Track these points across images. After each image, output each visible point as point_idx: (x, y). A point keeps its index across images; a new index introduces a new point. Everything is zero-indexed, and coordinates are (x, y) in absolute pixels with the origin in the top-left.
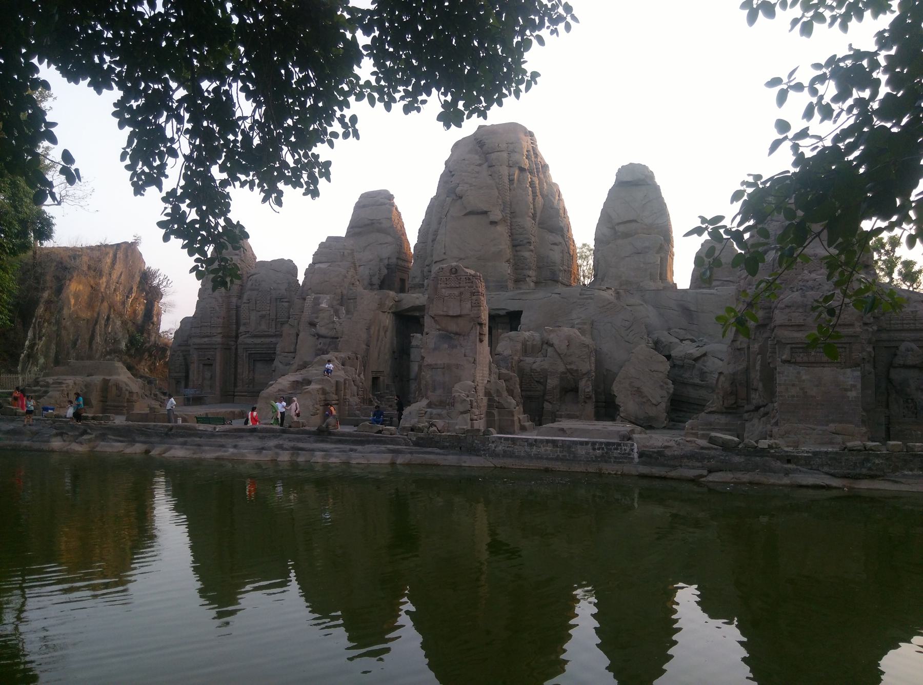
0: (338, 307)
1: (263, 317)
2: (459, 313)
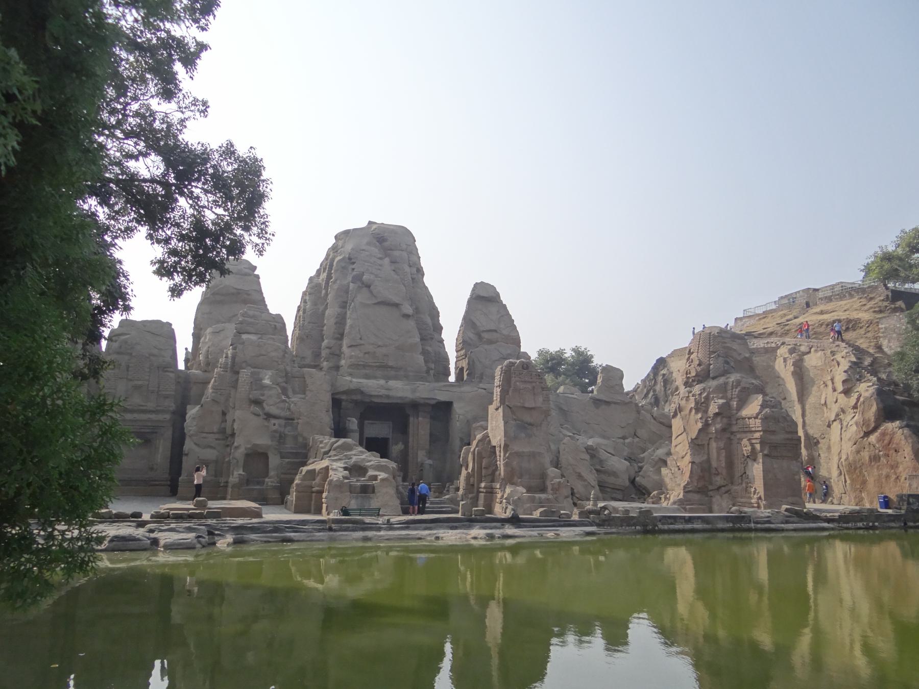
1: (137, 388)
2: (533, 405)
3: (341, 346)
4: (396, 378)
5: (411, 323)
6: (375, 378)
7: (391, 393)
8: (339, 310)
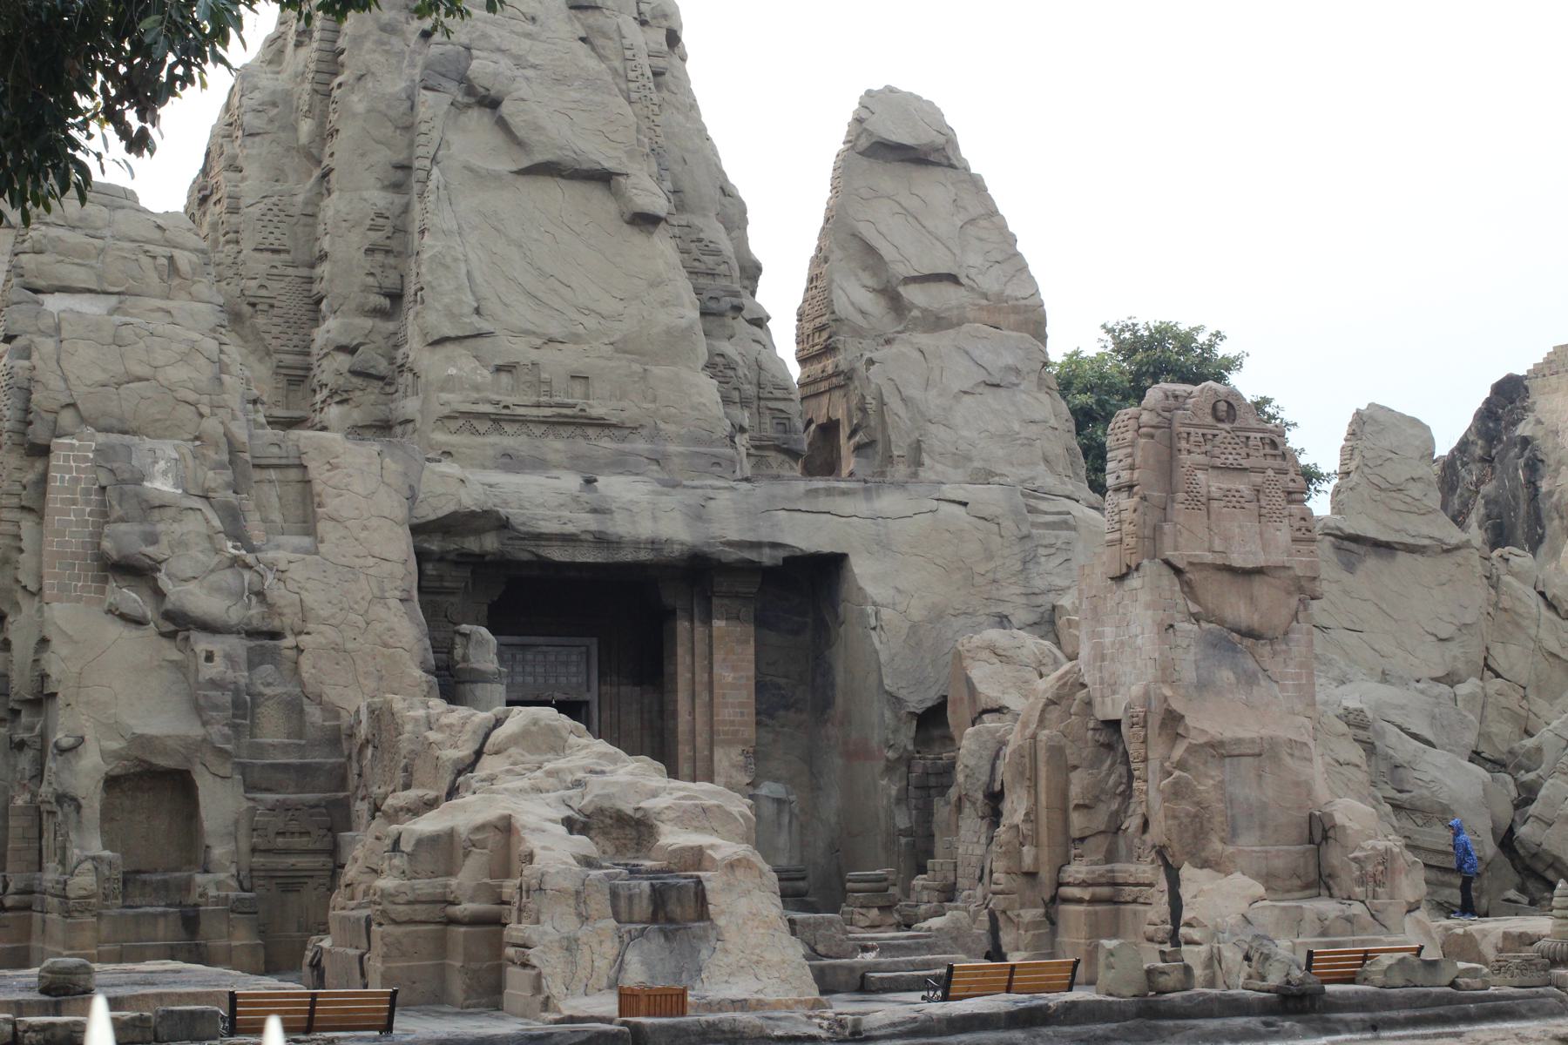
0: (230, 496)
3: (396, 342)
4: (620, 464)
5: (662, 249)
6: (539, 464)
7: (620, 526)
8: (380, 199)
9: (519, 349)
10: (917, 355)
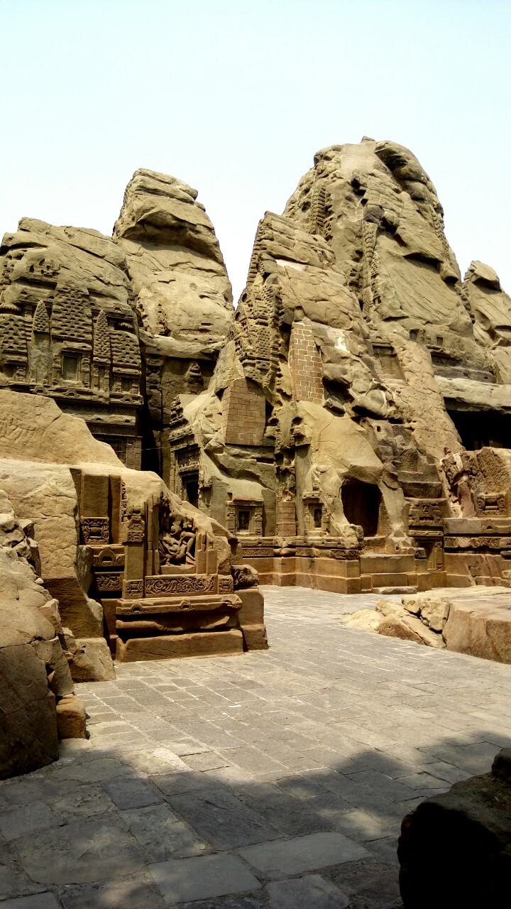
9: (418, 324)
10: (505, 353)
